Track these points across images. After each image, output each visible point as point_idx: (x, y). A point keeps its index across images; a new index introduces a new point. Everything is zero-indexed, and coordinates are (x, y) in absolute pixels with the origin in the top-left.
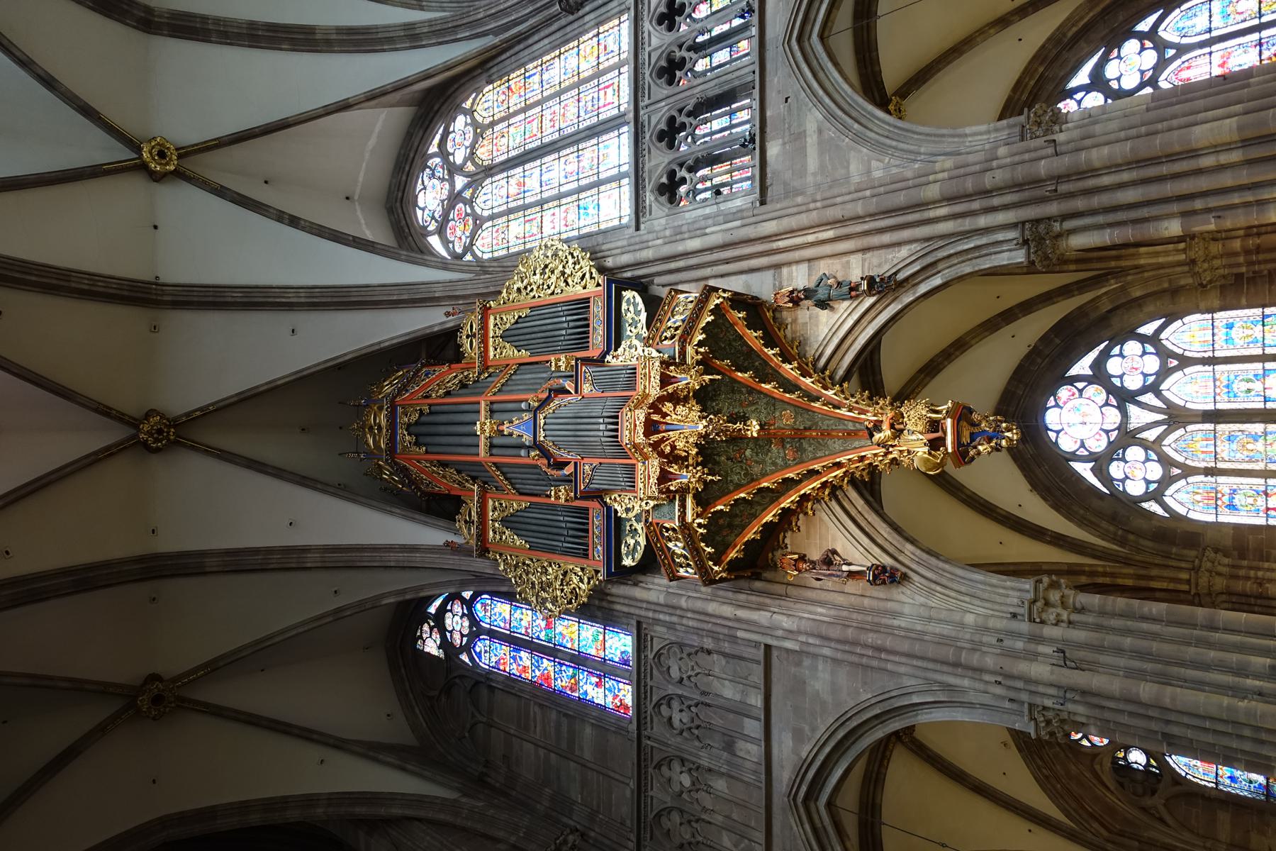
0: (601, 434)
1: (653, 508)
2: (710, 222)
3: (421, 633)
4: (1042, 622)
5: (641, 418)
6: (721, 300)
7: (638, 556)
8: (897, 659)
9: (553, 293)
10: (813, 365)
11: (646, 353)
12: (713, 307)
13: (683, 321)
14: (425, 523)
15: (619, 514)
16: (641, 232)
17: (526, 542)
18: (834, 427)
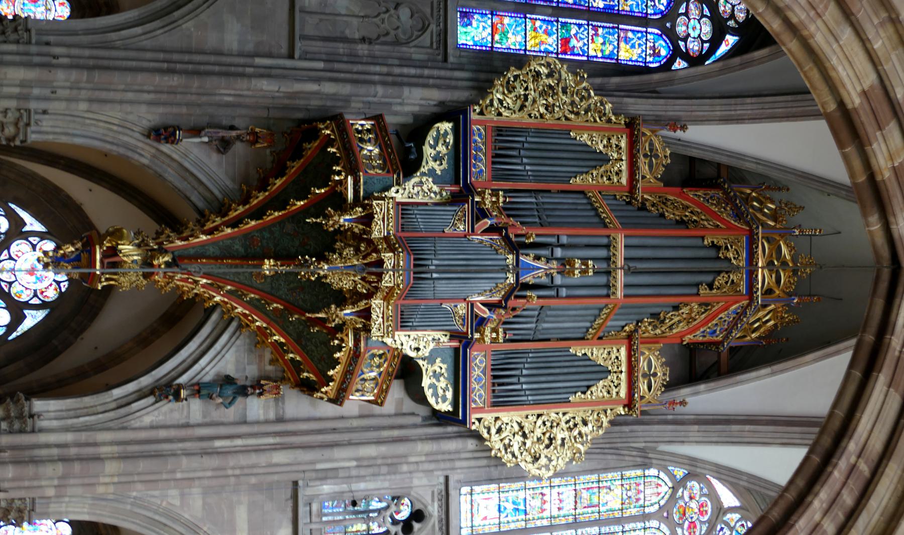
9: (539, 416)
17: (575, 139)
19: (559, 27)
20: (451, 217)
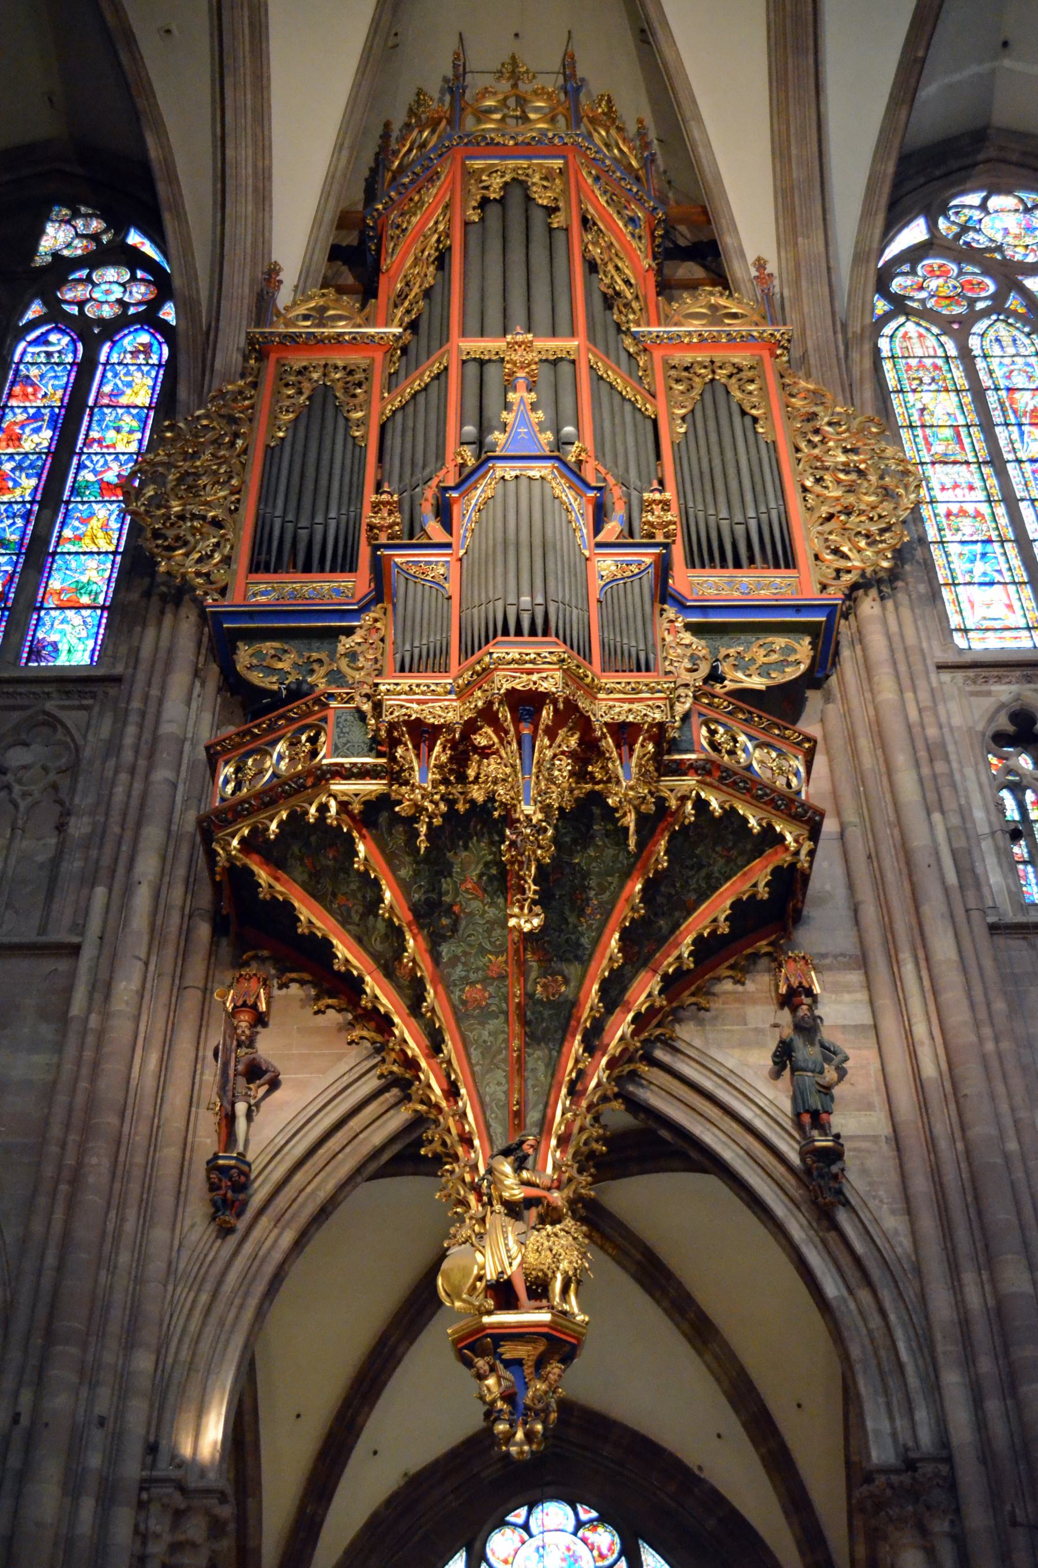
0: (512, 599)
1: (358, 710)
2: (955, 820)
3: (86, 216)
4: (142, 1505)
5: (545, 684)
6: (793, 846)
7: (257, 678)
8: (59, 1215)
9: (805, 489)
10: (658, 1038)
11: (682, 691)
12: (778, 829)
13: (749, 768)
14: (317, 222)
15: (343, 638)
16: (933, 676)
17: (282, 439)
18: (530, 1083)
19: (79, 499)
20: (419, 588)
